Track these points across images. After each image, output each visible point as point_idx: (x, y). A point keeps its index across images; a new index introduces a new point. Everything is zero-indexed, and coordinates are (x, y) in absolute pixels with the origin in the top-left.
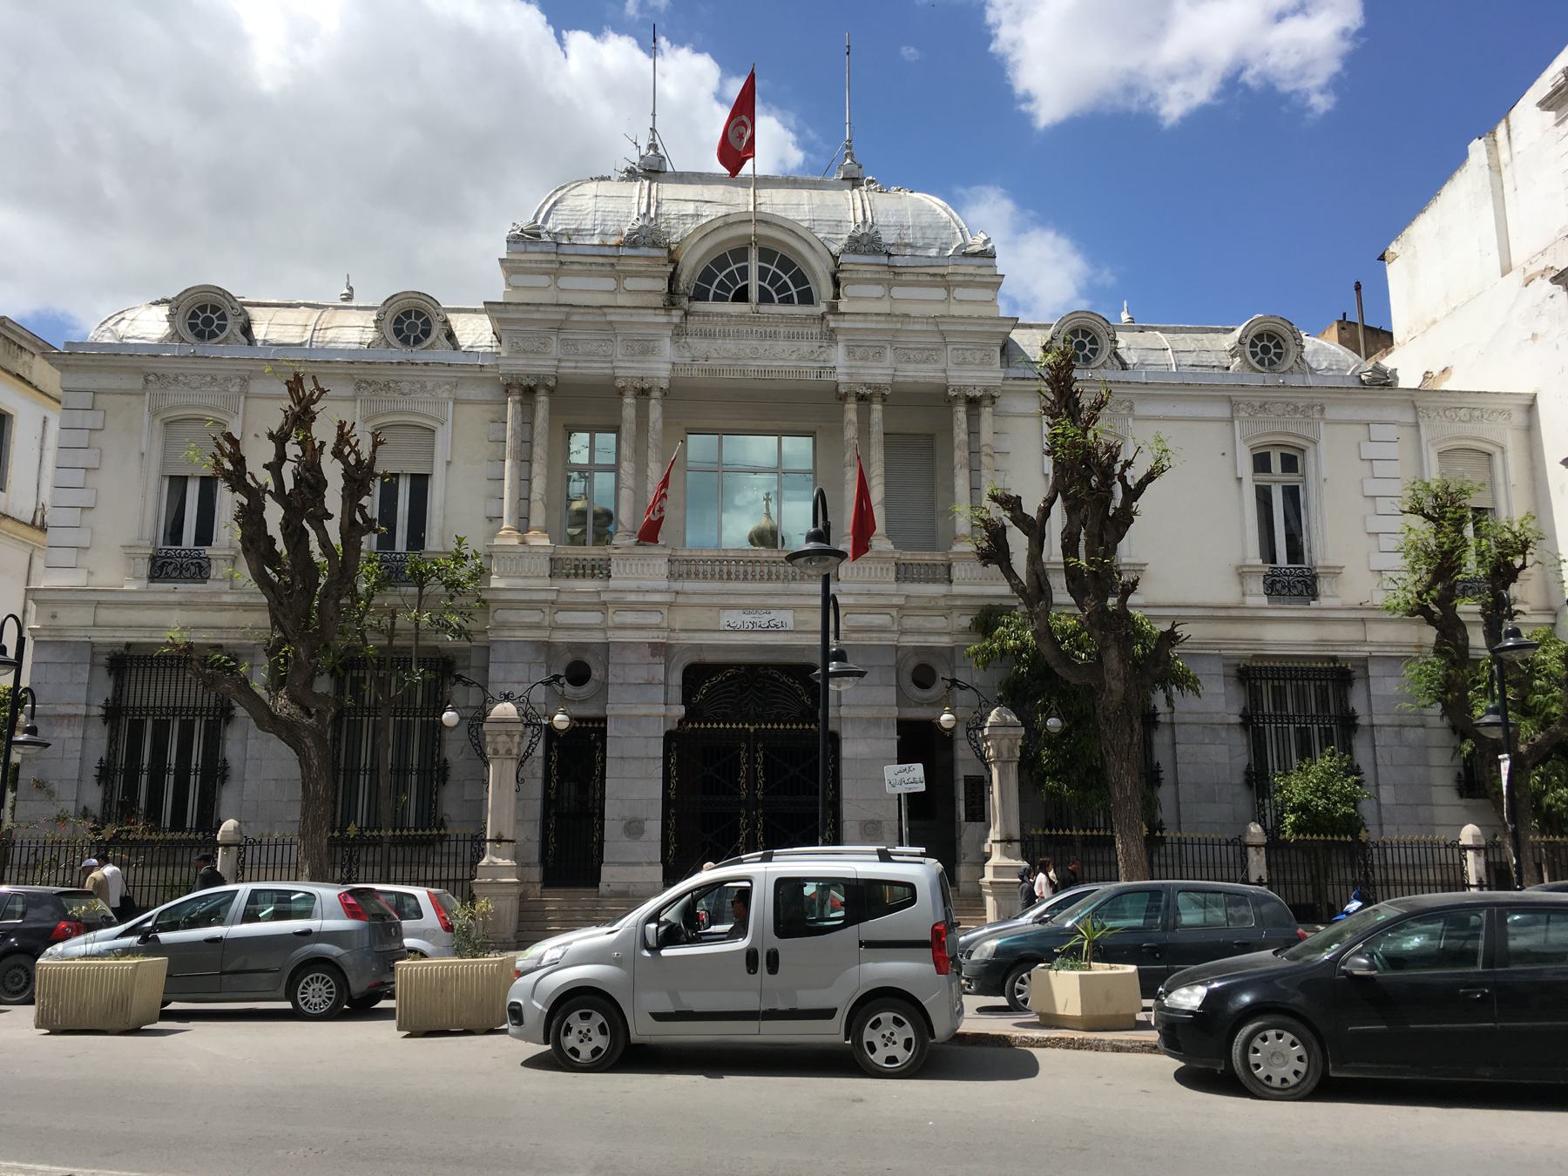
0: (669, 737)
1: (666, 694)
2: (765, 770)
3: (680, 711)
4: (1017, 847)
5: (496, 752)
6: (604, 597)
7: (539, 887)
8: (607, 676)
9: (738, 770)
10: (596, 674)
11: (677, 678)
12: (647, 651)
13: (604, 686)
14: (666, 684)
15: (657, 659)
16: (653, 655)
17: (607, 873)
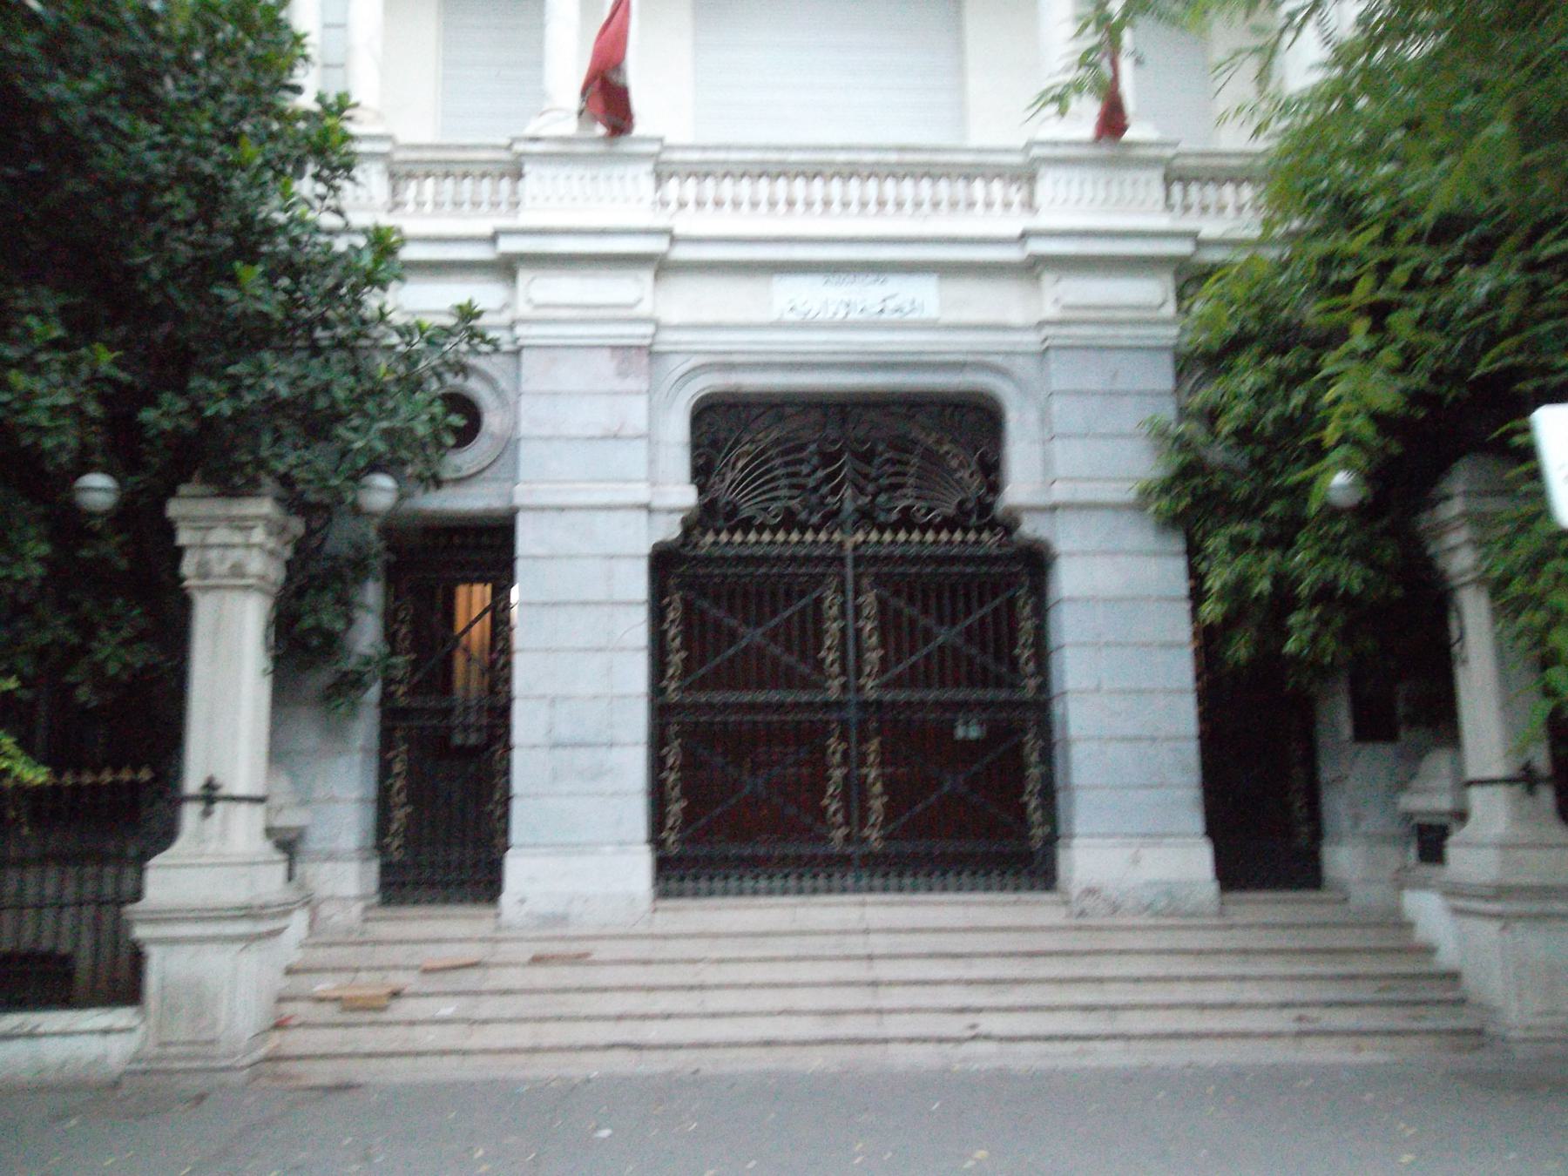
0: (663, 562)
1: (652, 462)
2: (882, 630)
3: (686, 496)
4: (1547, 795)
5: (204, 572)
6: (508, 245)
7: (357, 909)
8: (516, 424)
9: (819, 635)
10: (493, 421)
11: (677, 429)
12: (605, 364)
13: (509, 446)
14: (649, 437)
15: (632, 383)
16: (622, 374)
17: (517, 868)
